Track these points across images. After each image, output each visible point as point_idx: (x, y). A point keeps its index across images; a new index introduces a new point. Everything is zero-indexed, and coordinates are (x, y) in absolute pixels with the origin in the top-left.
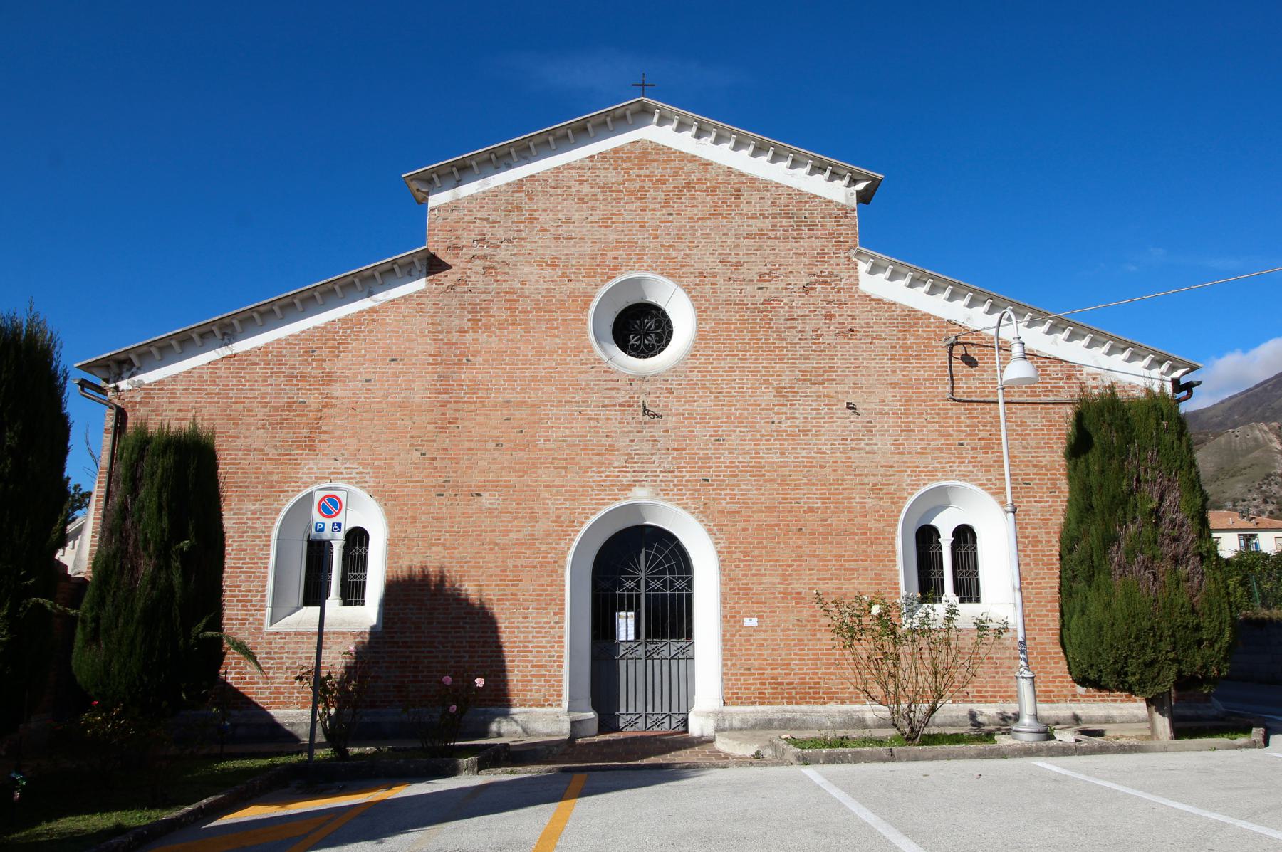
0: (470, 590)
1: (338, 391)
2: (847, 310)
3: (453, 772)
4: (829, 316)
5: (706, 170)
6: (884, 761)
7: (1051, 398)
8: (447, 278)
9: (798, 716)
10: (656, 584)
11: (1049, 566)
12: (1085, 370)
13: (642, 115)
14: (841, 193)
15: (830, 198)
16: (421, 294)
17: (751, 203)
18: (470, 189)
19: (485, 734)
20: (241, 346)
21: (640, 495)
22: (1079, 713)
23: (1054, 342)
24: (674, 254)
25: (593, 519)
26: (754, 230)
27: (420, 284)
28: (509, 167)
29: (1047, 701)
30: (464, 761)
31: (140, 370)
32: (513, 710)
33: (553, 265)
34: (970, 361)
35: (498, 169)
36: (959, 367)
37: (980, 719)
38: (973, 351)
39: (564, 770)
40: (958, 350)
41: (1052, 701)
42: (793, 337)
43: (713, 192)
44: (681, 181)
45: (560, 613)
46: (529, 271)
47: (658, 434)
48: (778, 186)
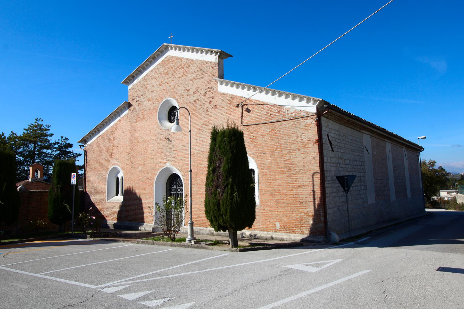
0: (137, 192)
1: (116, 142)
2: (215, 99)
3: (86, 238)
4: (210, 102)
5: (182, 61)
6: (151, 244)
7: (273, 120)
8: (132, 108)
9: (198, 230)
10: (179, 190)
11: (90, 181)
12: (285, 107)
13: (166, 49)
14: (214, 58)
15: (211, 61)
16: (127, 114)
17: (193, 68)
18: (136, 82)
19: (138, 230)
20: (101, 133)
21: (168, 165)
22: (273, 236)
23: (275, 99)
24: (174, 90)
25: (159, 172)
26: (192, 78)
27: (127, 111)
28: (142, 73)
29: (267, 231)
30: (88, 236)
31: (88, 141)
32: (145, 224)
33: (150, 100)
34: (248, 111)
35: (140, 74)
36: (245, 113)
37: (244, 235)
38: (249, 107)
39: (101, 240)
40: (245, 107)
41: (268, 231)
42: (201, 111)
43: (182, 68)
44: (176, 67)
45: (153, 199)
46: (146, 102)
47: (172, 146)
48: (199, 60)
